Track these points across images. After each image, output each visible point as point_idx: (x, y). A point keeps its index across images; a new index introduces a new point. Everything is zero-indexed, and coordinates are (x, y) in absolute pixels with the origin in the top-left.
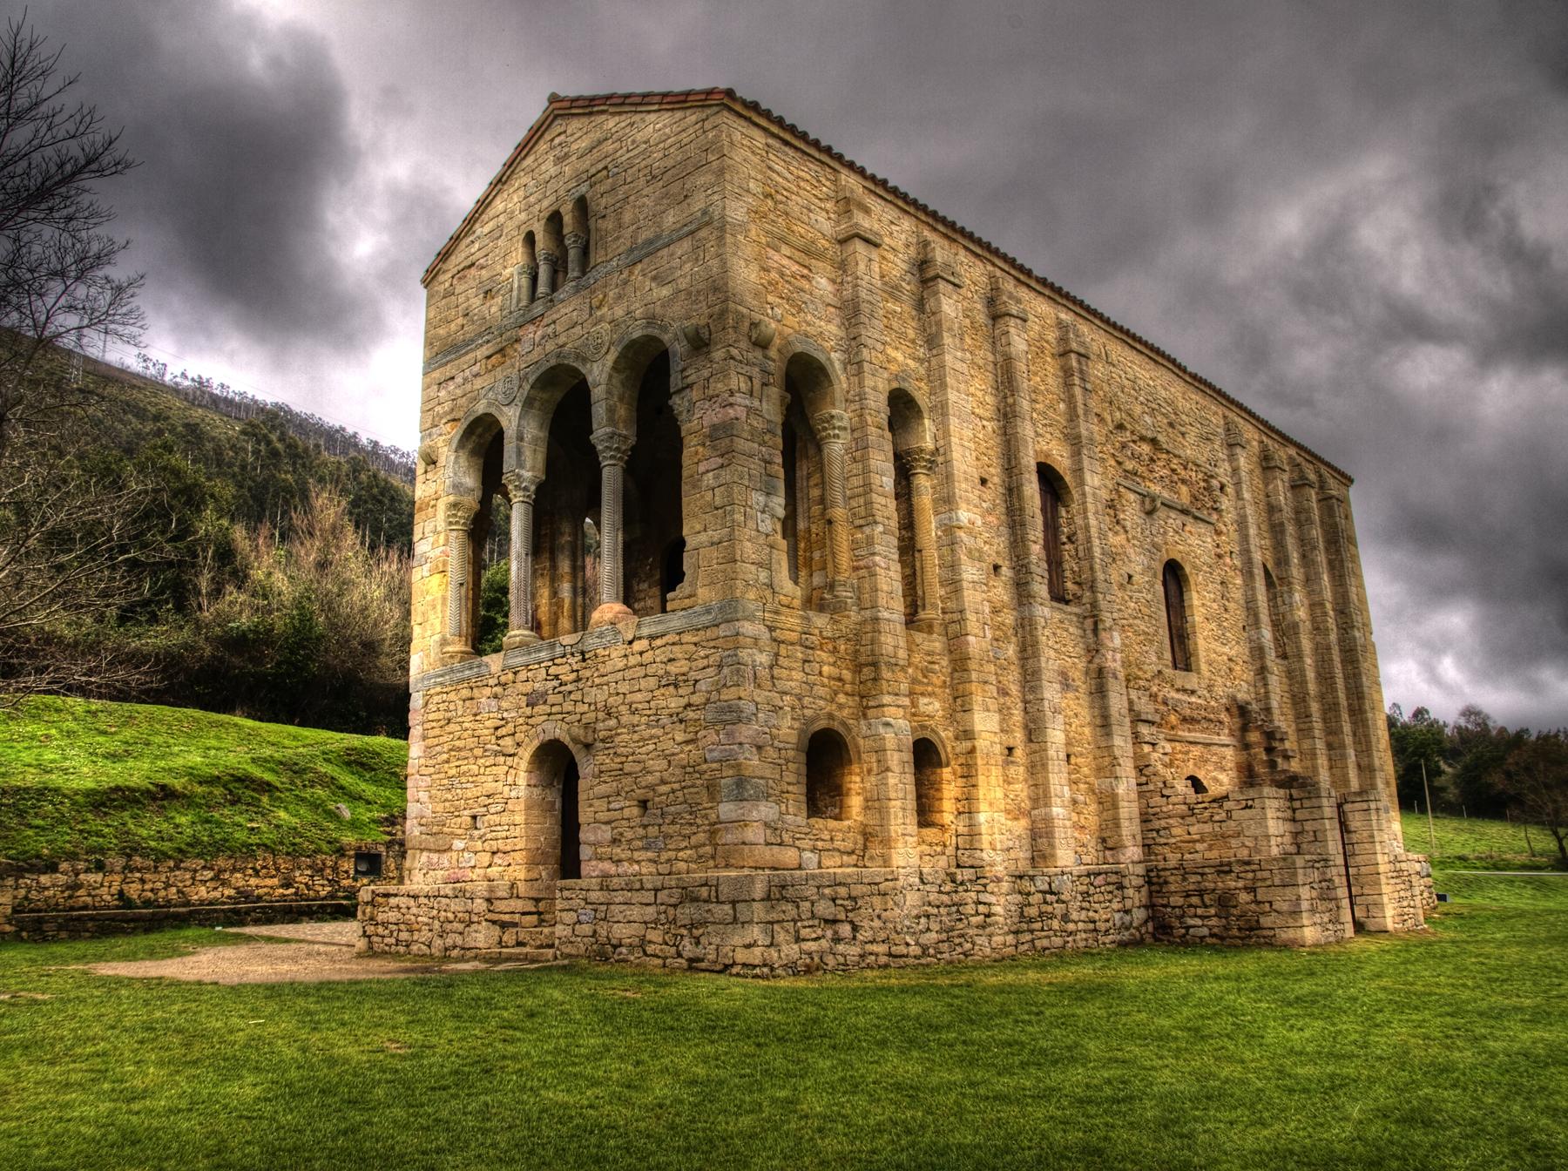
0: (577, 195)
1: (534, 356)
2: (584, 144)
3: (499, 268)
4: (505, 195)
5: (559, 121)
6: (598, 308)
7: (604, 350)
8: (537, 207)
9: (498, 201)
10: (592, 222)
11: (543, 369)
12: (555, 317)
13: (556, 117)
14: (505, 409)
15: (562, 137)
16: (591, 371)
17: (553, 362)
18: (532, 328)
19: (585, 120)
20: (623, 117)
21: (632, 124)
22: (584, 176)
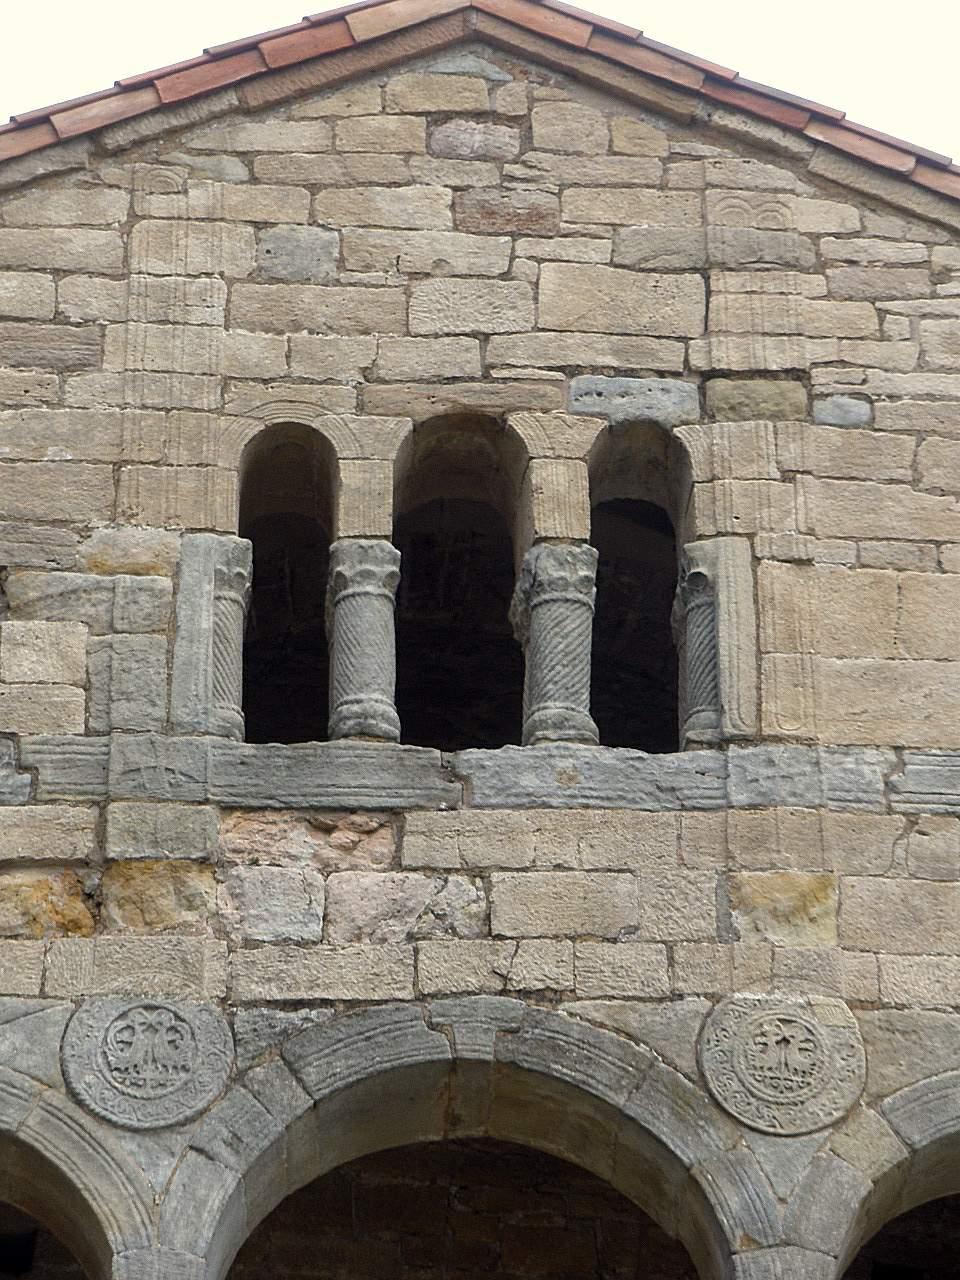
0: (623, 408)
1: (345, 974)
2: (658, 221)
3: (68, 499)
4: (115, 204)
5: (468, 62)
6: (784, 917)
7: (823, 1107)
8: (355, 352)
9: (60, 205)
10: (718, 555)
11: (381, 1059)
12: (480, 851)
13: (478, 39)
14: (125, 1147)
15: (505, 137)
16: (735, 1170)
17: (477, 1044)
18: (301, 840)
19: (655, 137)
20: (893, 224)
21: (943, 275)
22: (671, 356)
